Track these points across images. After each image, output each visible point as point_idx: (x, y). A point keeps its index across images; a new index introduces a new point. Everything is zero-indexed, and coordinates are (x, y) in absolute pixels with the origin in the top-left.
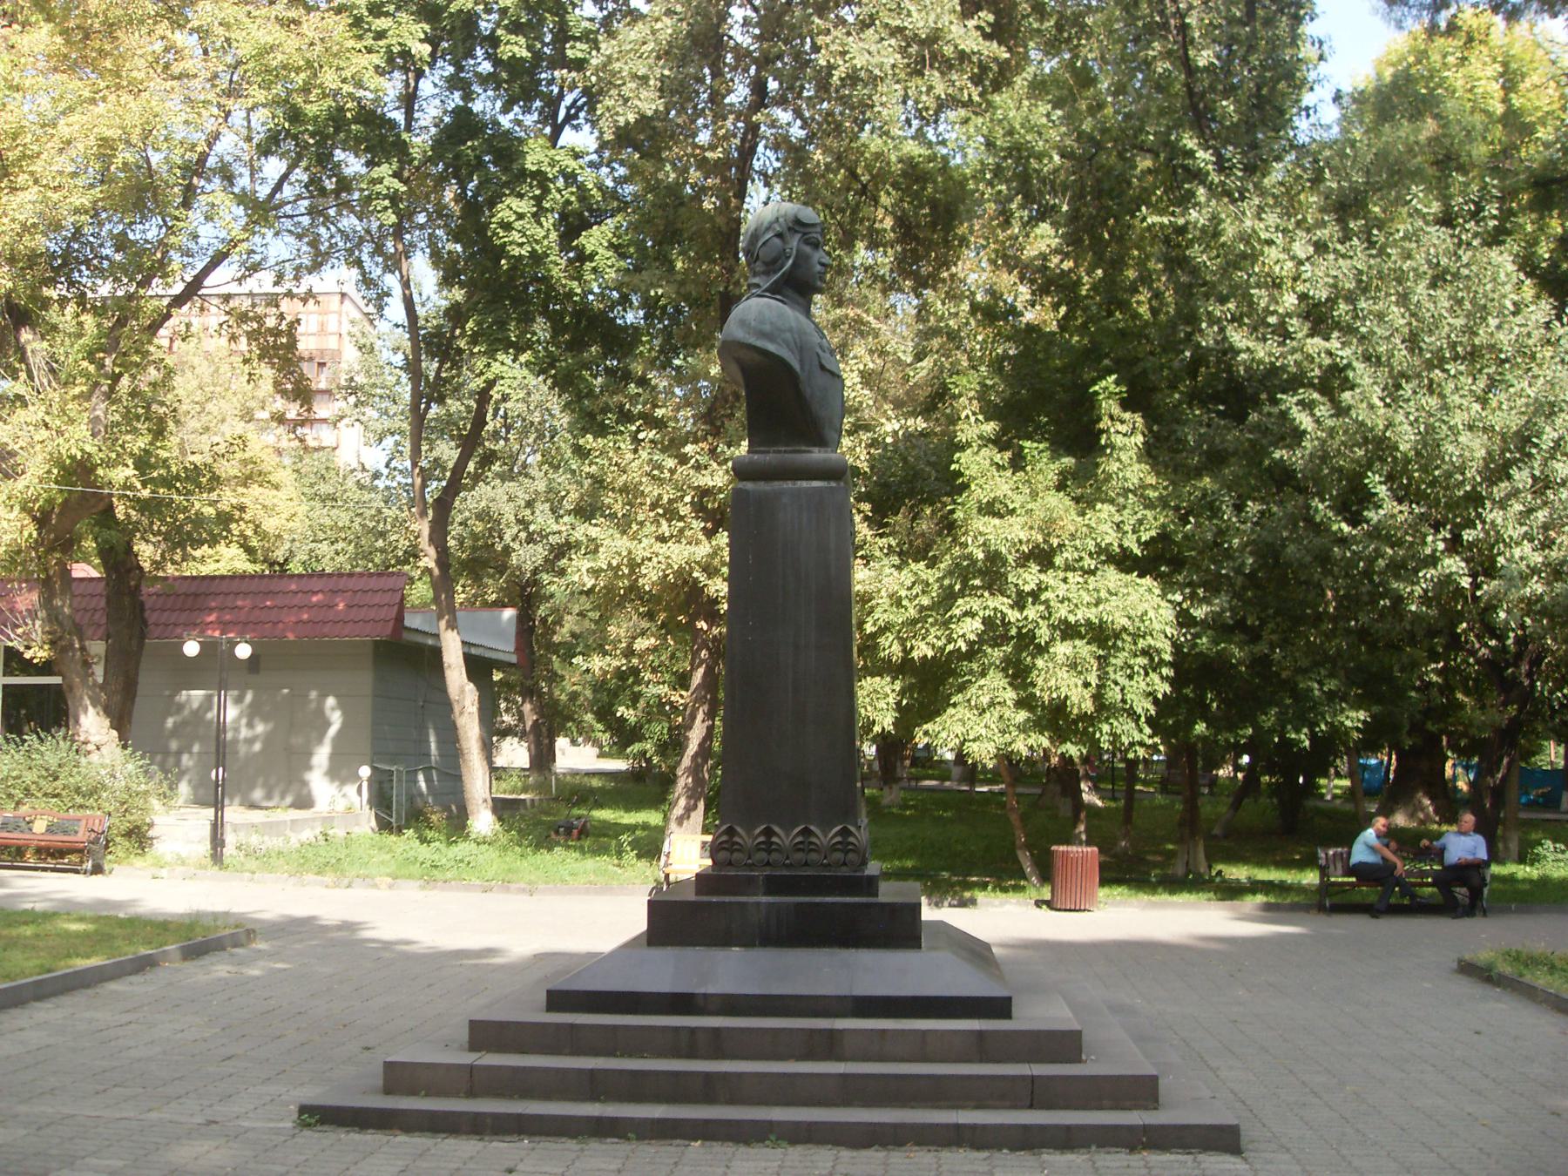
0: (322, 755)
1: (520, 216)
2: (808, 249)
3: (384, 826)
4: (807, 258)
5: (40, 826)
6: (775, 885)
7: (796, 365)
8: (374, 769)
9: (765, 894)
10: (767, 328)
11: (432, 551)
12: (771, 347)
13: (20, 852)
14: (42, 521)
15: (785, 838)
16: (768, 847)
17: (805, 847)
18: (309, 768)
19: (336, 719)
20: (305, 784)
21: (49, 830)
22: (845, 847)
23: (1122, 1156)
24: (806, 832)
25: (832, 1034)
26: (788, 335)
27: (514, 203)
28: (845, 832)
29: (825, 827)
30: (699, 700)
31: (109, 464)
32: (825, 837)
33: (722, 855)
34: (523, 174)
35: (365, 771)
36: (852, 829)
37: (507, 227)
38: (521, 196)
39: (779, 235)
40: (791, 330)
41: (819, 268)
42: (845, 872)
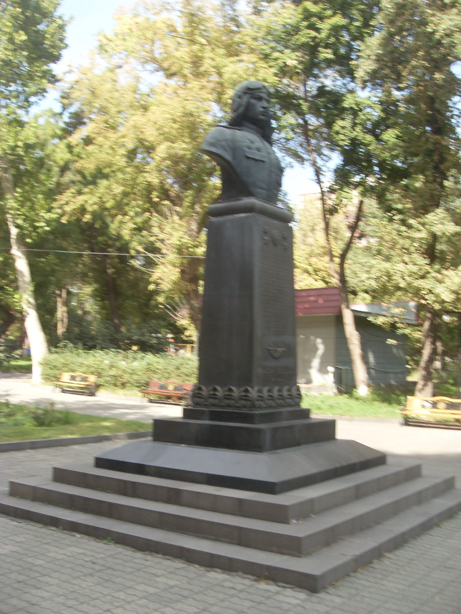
0: (316, 363)
1: (343, 128)
2: (253, 101)
3: (340, 392)
4: (253, 105)
5: (171, 388)
6: (214, 416)
7: (228, 157)
8: (336, 368)
9: (211, 419)
10: (212, 141)
11: (337, 276)
12: (213, 150)
13: (169, 397)
14: (183, 272)
15: (220, 392)
16: (214, 397)
17: (228, 397)
18: (310, 367)
19: (321, 349)
20: (309, 374)
21: (176, 389)
22: (245, 398)
23: (247, 582)
24: (230, 390)
25: (178, 492)
26: (224, 143)
27: (340, 123)
28: (247, 391)
29: (238, 386)
30: (427, 336)
31: (196, 246)
32: (236, 392)
33: (197, 399)
34: (344, 109)
35: (331, 369)
36: (249, 388)
37: (337, 133)
38: (343, 119)
39: (240, 97)
40: (226, 140)
41: (262, 109)
42: (245, 411)
